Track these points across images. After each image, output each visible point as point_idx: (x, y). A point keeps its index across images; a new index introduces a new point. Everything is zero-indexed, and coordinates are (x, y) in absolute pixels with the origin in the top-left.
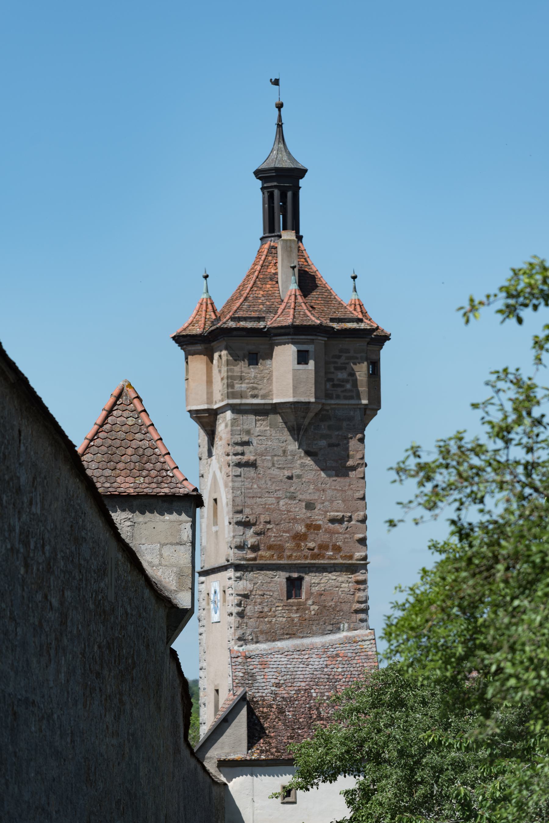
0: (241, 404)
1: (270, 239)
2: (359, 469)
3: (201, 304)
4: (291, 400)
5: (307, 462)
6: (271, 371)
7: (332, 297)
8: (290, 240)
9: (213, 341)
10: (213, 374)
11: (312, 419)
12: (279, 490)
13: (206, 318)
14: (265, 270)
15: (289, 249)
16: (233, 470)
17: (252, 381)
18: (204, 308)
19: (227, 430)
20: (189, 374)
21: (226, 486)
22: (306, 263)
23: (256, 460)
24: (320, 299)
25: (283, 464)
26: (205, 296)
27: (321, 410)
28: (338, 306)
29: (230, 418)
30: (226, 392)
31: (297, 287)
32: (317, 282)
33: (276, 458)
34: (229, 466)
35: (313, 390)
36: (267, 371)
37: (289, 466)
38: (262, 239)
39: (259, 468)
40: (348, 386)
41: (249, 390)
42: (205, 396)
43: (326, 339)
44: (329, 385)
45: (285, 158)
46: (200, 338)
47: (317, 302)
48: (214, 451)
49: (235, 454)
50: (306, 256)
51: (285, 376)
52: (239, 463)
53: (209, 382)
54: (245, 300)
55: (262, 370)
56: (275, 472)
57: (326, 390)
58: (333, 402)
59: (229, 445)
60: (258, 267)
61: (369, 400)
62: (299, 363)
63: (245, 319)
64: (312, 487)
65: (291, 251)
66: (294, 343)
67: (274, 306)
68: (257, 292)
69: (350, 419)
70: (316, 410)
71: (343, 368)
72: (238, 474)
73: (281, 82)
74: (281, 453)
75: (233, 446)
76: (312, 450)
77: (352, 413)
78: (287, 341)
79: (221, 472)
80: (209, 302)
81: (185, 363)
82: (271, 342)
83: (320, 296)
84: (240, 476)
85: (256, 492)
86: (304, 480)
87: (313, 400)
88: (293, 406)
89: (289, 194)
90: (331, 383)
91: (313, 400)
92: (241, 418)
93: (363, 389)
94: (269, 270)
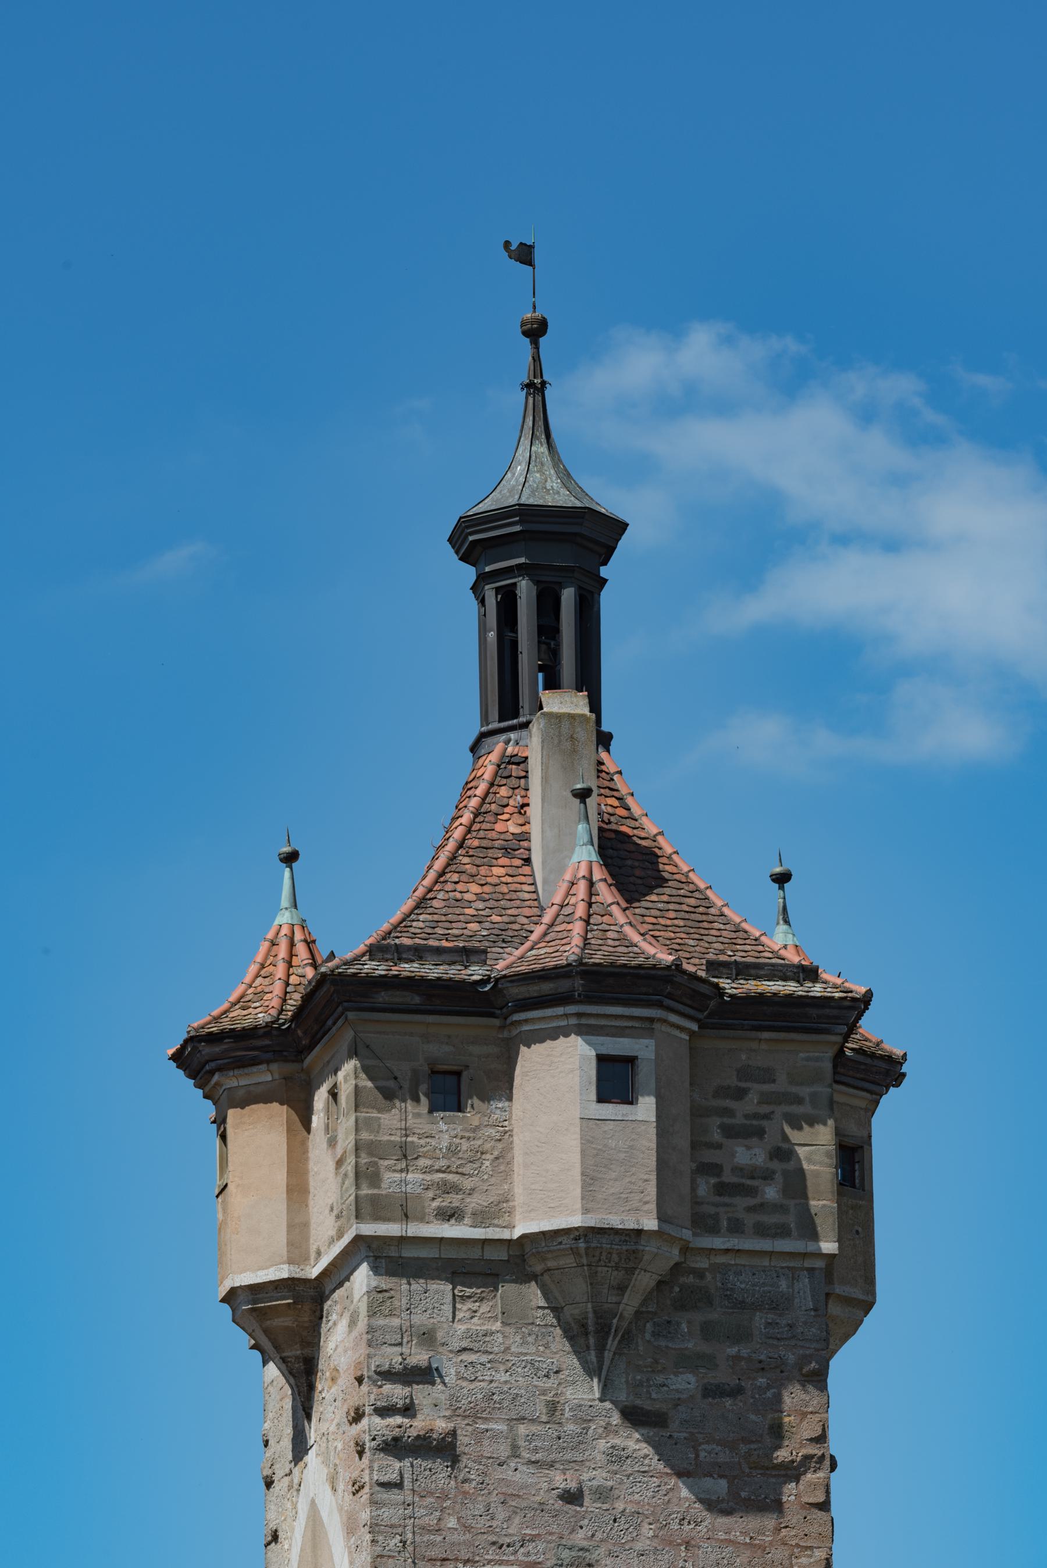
0: (402, 1240)
1: (503, 737)
2: (809, 1475)
3: (273, 943)
4: (575, 1220)
5: (632, 1445)
6: (508, 1133)
7: (712, 911)
8: (572, 717)
9: (311, 1048)
10: (313, 1167)
11: (645, 1302)
12: (533, 1539)
13: (287, 984)
14: (484, 826)
15: (568, 745)
16: (376, 1466)
17: (443, 1163)
18: (282, 952)
19: (355, 1333)
20: (230, 1167)
21: (350, 1530)
22: (622, 812)
23: (454, 1433)
24: (672, 915)
25: (549, 1450)
26: (284, 918)
27: (677, 1268)
28: (734, 935)
29: (365, 1289)
30: (353, 1197)
31: (594, 857)
32: (661, 866)
33: (522, 1429)
34: (361, 1453)
35: (652, 1190)
36: (492, 1131)
37: (568, 1457)
38: (474, 749)
39: (464, 1459)
40: (771, 1193)
41: (430, 1194)
42: (281, 1238)
43: (695, 1027)
44: (704, 1189)
45: (554, 483)
46: (267, 1042)
47: (662, 921)
48: (312, 1436)
49: (383, 1412)
50: (624, 791)
51: (558, 1145)
52: (396, 1439)
53: (298, 1189)
54: (417, 907)
55: (476, 1129)
56: (521, 1475)
57: (696, 1202)
58: (718, 1242)
59: (360, 1380)
60: (467, 817)
61: (839, 1241)
62: (601, 1099)
63: (419, 953)
64: (647, 1531)
65: (574, 751)
66: (583, 1031)
67: (516, 927)
68: (460, 887)
69: (778, 1304)
70: (663, 1266)
71: (752, 1132)
72: (394, 1477)
73: (538, 256)
74: (540, 1410)
75: (374, 1382)
76: (647, 1406)
77: (783, 1285)
78: (563, 1023)
79: (334, 1489)
80: (298, 936)
81: (218, 1141)
82: (506, 1034)
83: (671, 906)
84: (399, 1485)
85: (453, 1544)
86: (620, 1506)
87: (651, 1224)
88: (582, 1245)
89: (568, 596)
90: (713, 1181)
91: (651, 1224)
92: (405, 1287)
93: (822, 1203)
94: (499, 827)
